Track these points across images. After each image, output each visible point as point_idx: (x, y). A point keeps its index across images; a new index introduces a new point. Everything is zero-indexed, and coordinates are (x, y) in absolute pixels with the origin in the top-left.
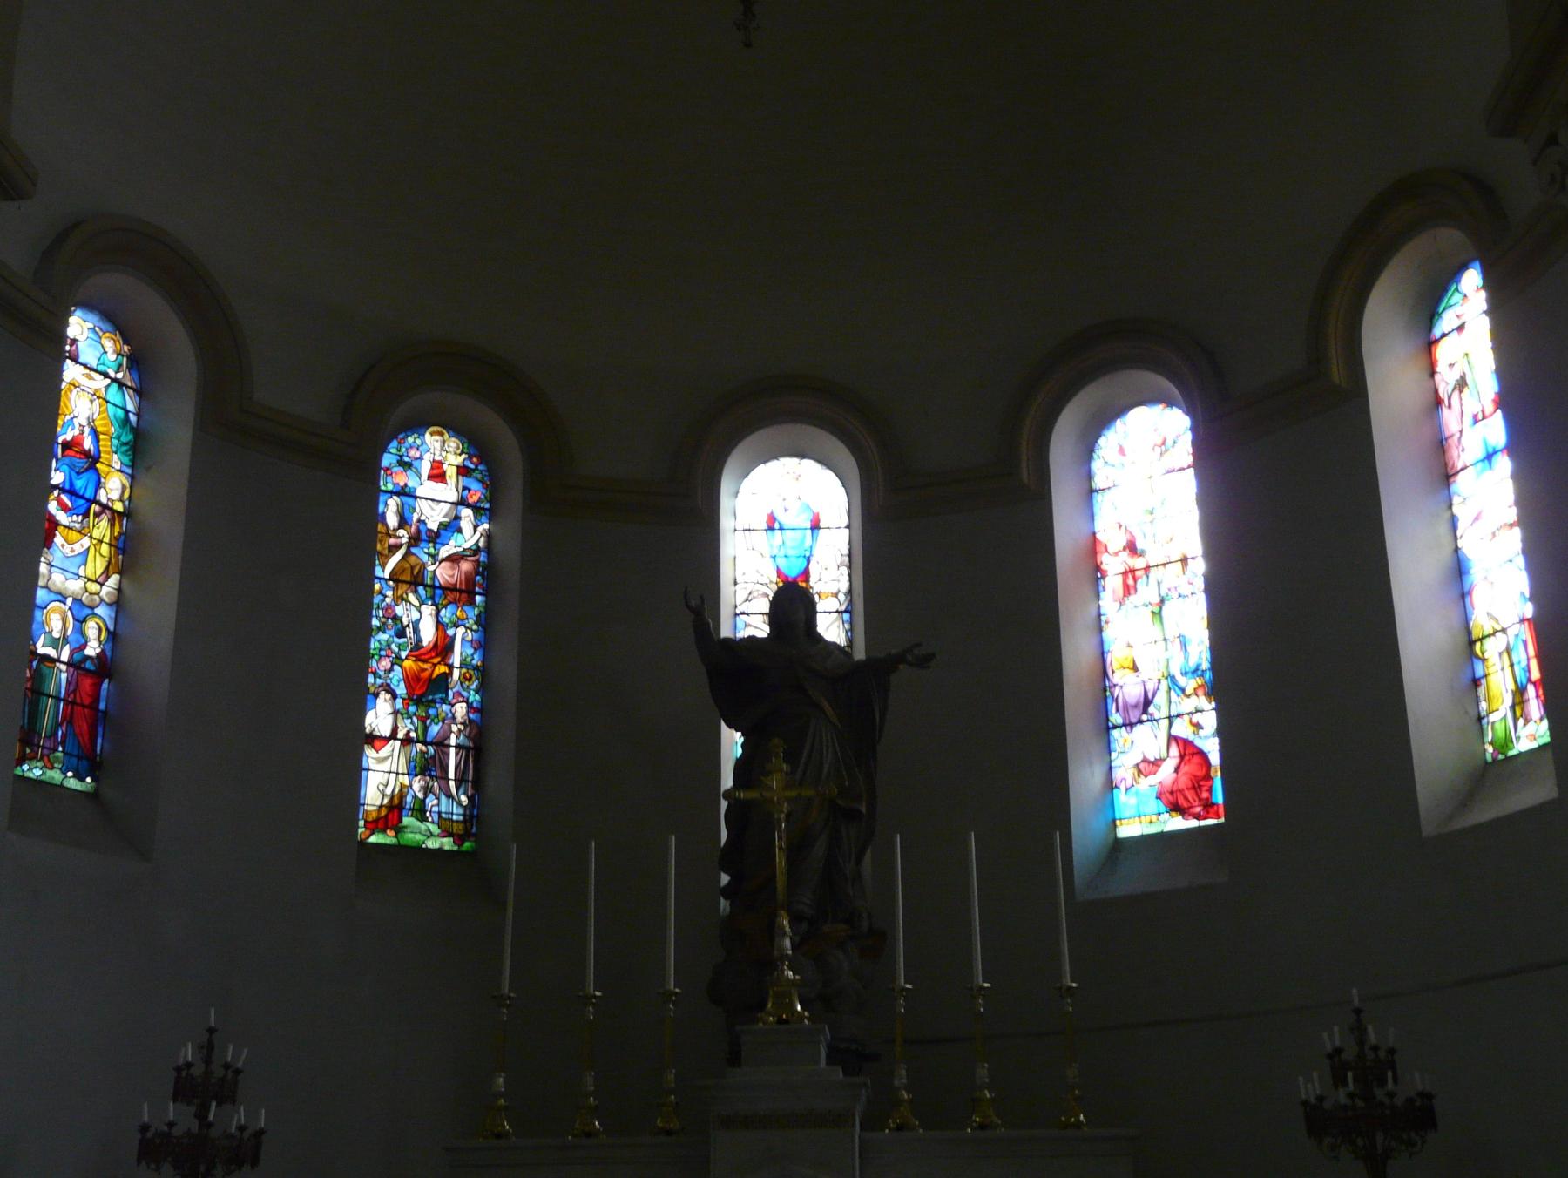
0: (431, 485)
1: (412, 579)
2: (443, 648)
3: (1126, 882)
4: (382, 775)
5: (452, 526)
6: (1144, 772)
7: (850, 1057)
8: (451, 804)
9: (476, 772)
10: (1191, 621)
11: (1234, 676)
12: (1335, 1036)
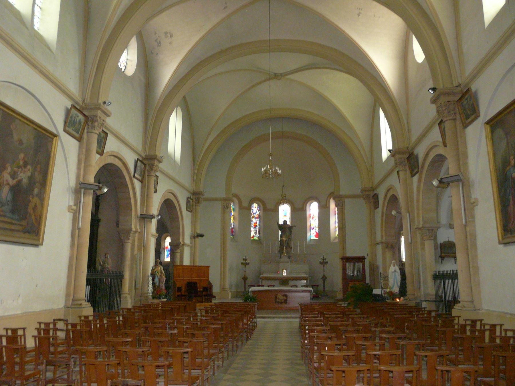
0: (255, 208)
1: (254, 217)
2: (256, 223)
3: (312, 243)
4: (253, 234)
6: (312, 235)
7: (289, 257)
8: (257, 236)
9: (259, 234)
11: (320, 226)
12: (322, 257)
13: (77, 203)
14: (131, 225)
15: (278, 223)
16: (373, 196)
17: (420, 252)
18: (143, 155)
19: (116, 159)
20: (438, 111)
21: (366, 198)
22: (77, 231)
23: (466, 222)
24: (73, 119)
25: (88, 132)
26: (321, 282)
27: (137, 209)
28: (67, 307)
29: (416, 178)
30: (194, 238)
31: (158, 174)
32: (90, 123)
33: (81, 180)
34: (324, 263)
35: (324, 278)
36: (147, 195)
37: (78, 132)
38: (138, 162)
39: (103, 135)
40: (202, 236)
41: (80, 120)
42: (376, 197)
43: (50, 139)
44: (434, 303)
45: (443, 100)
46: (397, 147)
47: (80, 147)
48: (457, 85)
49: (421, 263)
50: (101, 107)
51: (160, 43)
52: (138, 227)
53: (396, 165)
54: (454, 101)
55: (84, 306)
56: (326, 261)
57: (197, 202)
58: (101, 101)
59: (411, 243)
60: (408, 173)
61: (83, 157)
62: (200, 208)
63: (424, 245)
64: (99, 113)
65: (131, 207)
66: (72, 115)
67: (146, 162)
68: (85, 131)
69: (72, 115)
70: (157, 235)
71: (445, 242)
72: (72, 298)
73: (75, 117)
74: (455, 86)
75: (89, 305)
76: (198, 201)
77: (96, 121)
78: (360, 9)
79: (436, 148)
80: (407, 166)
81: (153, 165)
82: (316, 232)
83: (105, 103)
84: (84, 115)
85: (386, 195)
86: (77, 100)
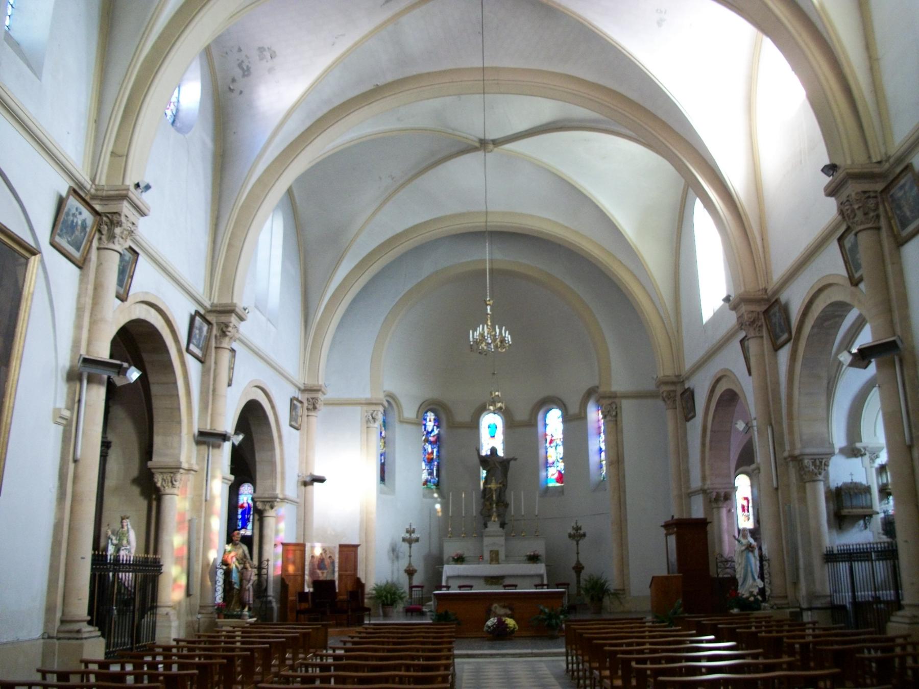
2: (432, 453)
5: (433, 430)
7: (503, 525)
10: (561, 449)
12: (573, 524)
13: (75, 403)
14: (180, 454)
15: (478, 451)
16: (682, 394)
17: (797, 506)
18: (208, 304)
19: (153, 311)
20: (841, 212)
21: (669, 398)
22: (72, 466)
23: (911, 438)
24: (71, 218)
25: (98, 249)
26: (573, 574)
27: (191, 420)
28: (49, 637)
29: (784, 354)
30: (305, 484)
31: (235, 345)
32: (105, 228)
33: (83, 352)
34: (577, 535)
35: (578, 568)
36: (214, 390)
37: (78, 249)
38: (198, 319)
39: (128, 256)
40: (321, 480)
41: (84, 221)
42: (689, 396)
43: (23, 260)
44: (829, 611)
45: (852, 189)
46: (743, 289)
47: (83, 280)
48: (879, 159)
49: (799, 529)
50: (130, 194)
51: (248, 69)
52: (194, 461)
53: (741, 325)
54: (876, 192)
55: (85, 635)
56: (582, 532)
57: (311, 407)
58: (130, 182)
59: (777, 489)
60: (766, 343)
61: (88, 301)
62: (316, 421)
63: (805, 492)
64: (126, 208)
65: (180, 416)
66: (69, 210)
67: (210, 318)
68: (95, 244)
69: (69, 210)
70: (232, 477)
71: (845, 484)
72: (59, 615)
73: (74, 215)
74: (874, 160)
75: (94, 631)
76: (313, 406)
77: (119, 224)
78: (661, 12)
79: (826, 292)
80: (764, 329)
81: (227, 326)
82: (560, 472)
83: (137, 186)
84: (96, 213)
85: (712, 391)
86: (82, 181)
